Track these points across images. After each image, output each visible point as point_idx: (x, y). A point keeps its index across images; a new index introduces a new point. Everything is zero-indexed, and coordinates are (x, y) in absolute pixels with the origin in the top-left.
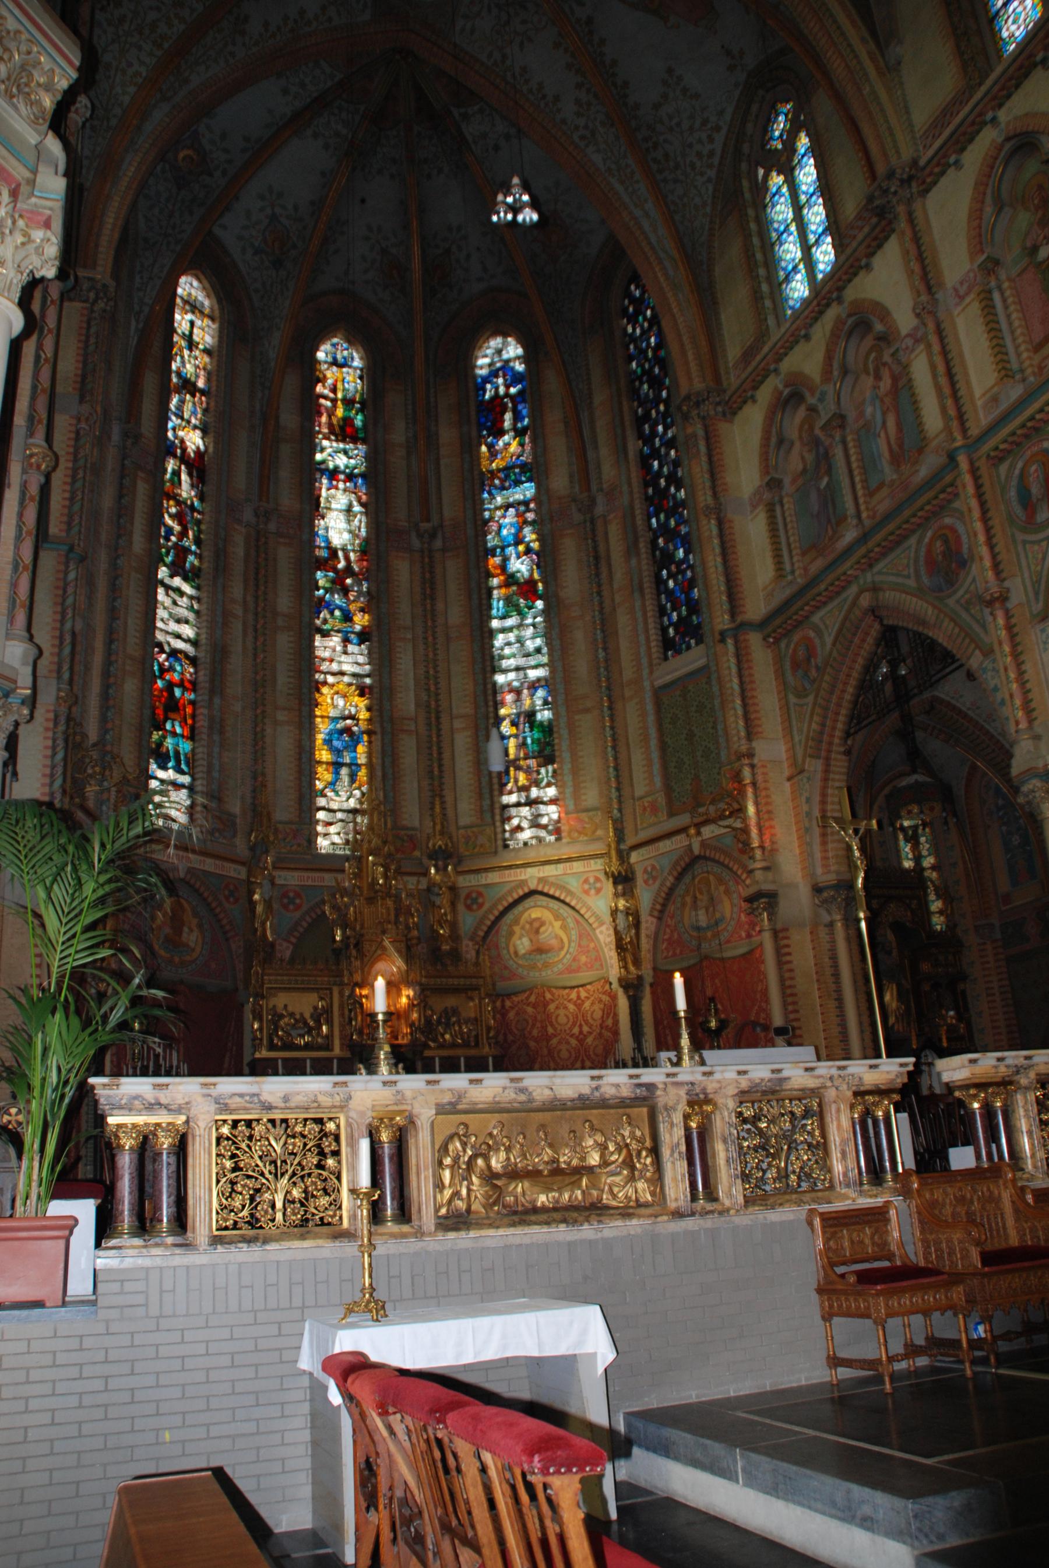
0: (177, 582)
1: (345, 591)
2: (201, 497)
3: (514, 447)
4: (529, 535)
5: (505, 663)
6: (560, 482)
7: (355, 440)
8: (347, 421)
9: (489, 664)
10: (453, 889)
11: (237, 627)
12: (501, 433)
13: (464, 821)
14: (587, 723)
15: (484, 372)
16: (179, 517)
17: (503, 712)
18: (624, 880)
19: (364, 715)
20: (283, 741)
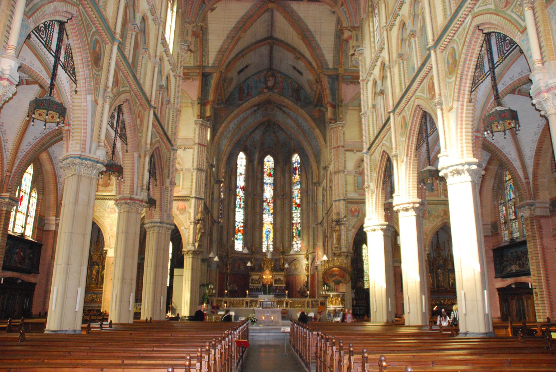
0: (240, 210)
1: (269, 206)
2: (244, 194)
3: (298, 178)
4: (299, 195)
6: (304, 185)
8: (270, 173)
9: (291, 218)
10: (284, 258)
11: (249, 216)
12: (295, 174)
13: (286, 246)
14: (305, 232)
15: (294, 161)
16: (240, 199)
18: (308, 259)
19: (272, 228)
20: (257, 234)
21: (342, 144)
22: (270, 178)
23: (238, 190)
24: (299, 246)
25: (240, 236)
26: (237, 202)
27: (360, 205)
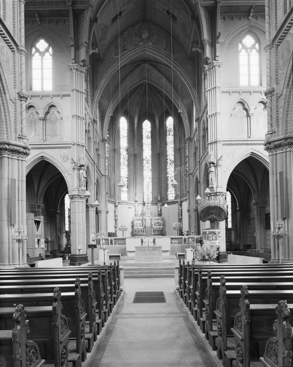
0: (124, 167)
5: (169, 173)
7: (149, 138)
9: (166, 173)
17: (169, 180)
22: (148, 140)
23: (121, 150)
24: (174, 195)
25: (125, 189)
26: (121, 160)
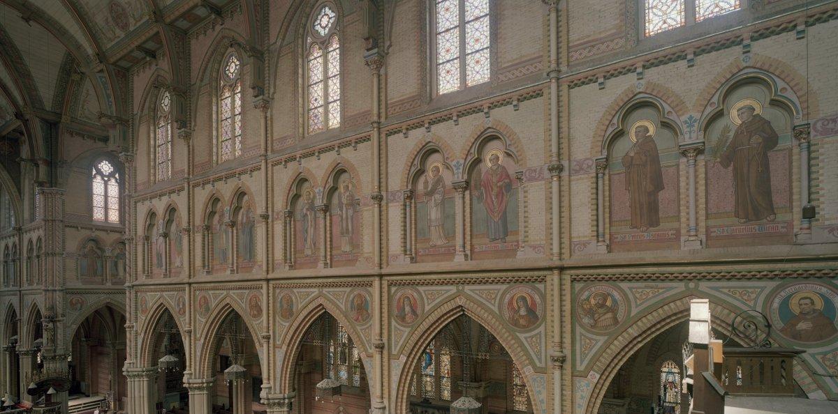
21: (60, 218)
27: (85, 295)
